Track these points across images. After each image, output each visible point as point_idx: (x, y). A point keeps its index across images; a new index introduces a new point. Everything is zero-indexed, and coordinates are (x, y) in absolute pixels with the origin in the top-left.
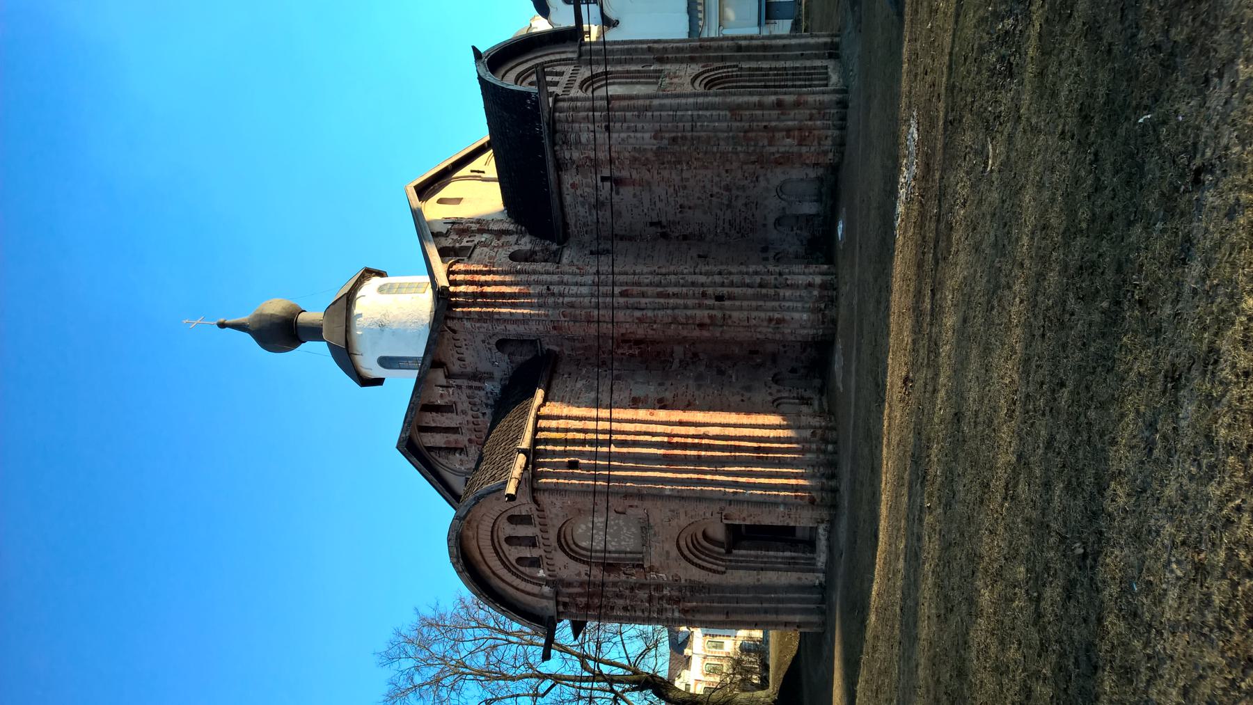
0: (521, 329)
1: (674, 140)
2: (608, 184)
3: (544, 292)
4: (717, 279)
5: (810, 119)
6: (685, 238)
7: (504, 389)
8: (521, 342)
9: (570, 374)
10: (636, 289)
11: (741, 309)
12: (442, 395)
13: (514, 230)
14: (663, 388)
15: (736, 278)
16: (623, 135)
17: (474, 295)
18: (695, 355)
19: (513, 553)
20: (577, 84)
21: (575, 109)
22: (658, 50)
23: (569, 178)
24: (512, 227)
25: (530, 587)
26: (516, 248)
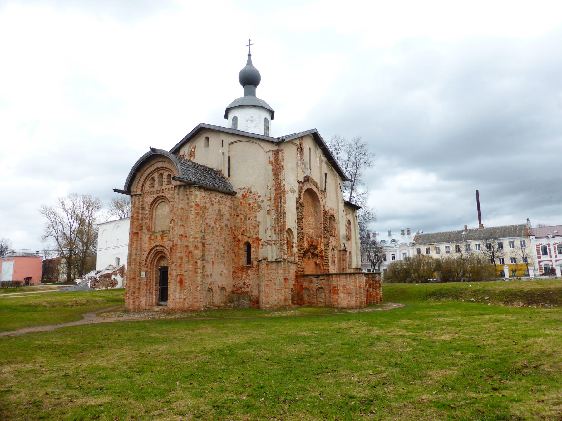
20: (160, 195)
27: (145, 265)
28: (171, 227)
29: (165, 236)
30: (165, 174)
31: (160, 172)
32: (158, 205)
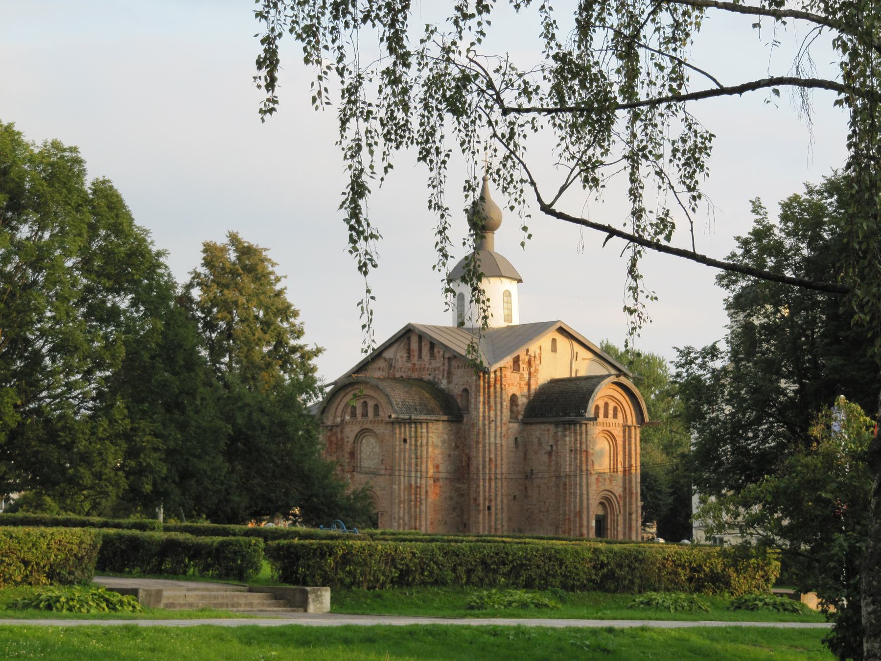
0: (473, 406)
1: (565, 484)
2: (549, 448)
4: (499, 507)
6: (526, 488)
7: (442, 391)
8: (468, 401)
10: (493, 466)
11: (484, 519)
12: (439, 352)
15: (499, 516)
16: (568, 459)
17: (489, 382)
18: (463, 495)
19: (358, 404)
20: (606, 428)
21: (581, 434)
23: (552, 428)
24: (532, 391)
25: (339, 411)
30: (612, 405)
31: (606, 400)
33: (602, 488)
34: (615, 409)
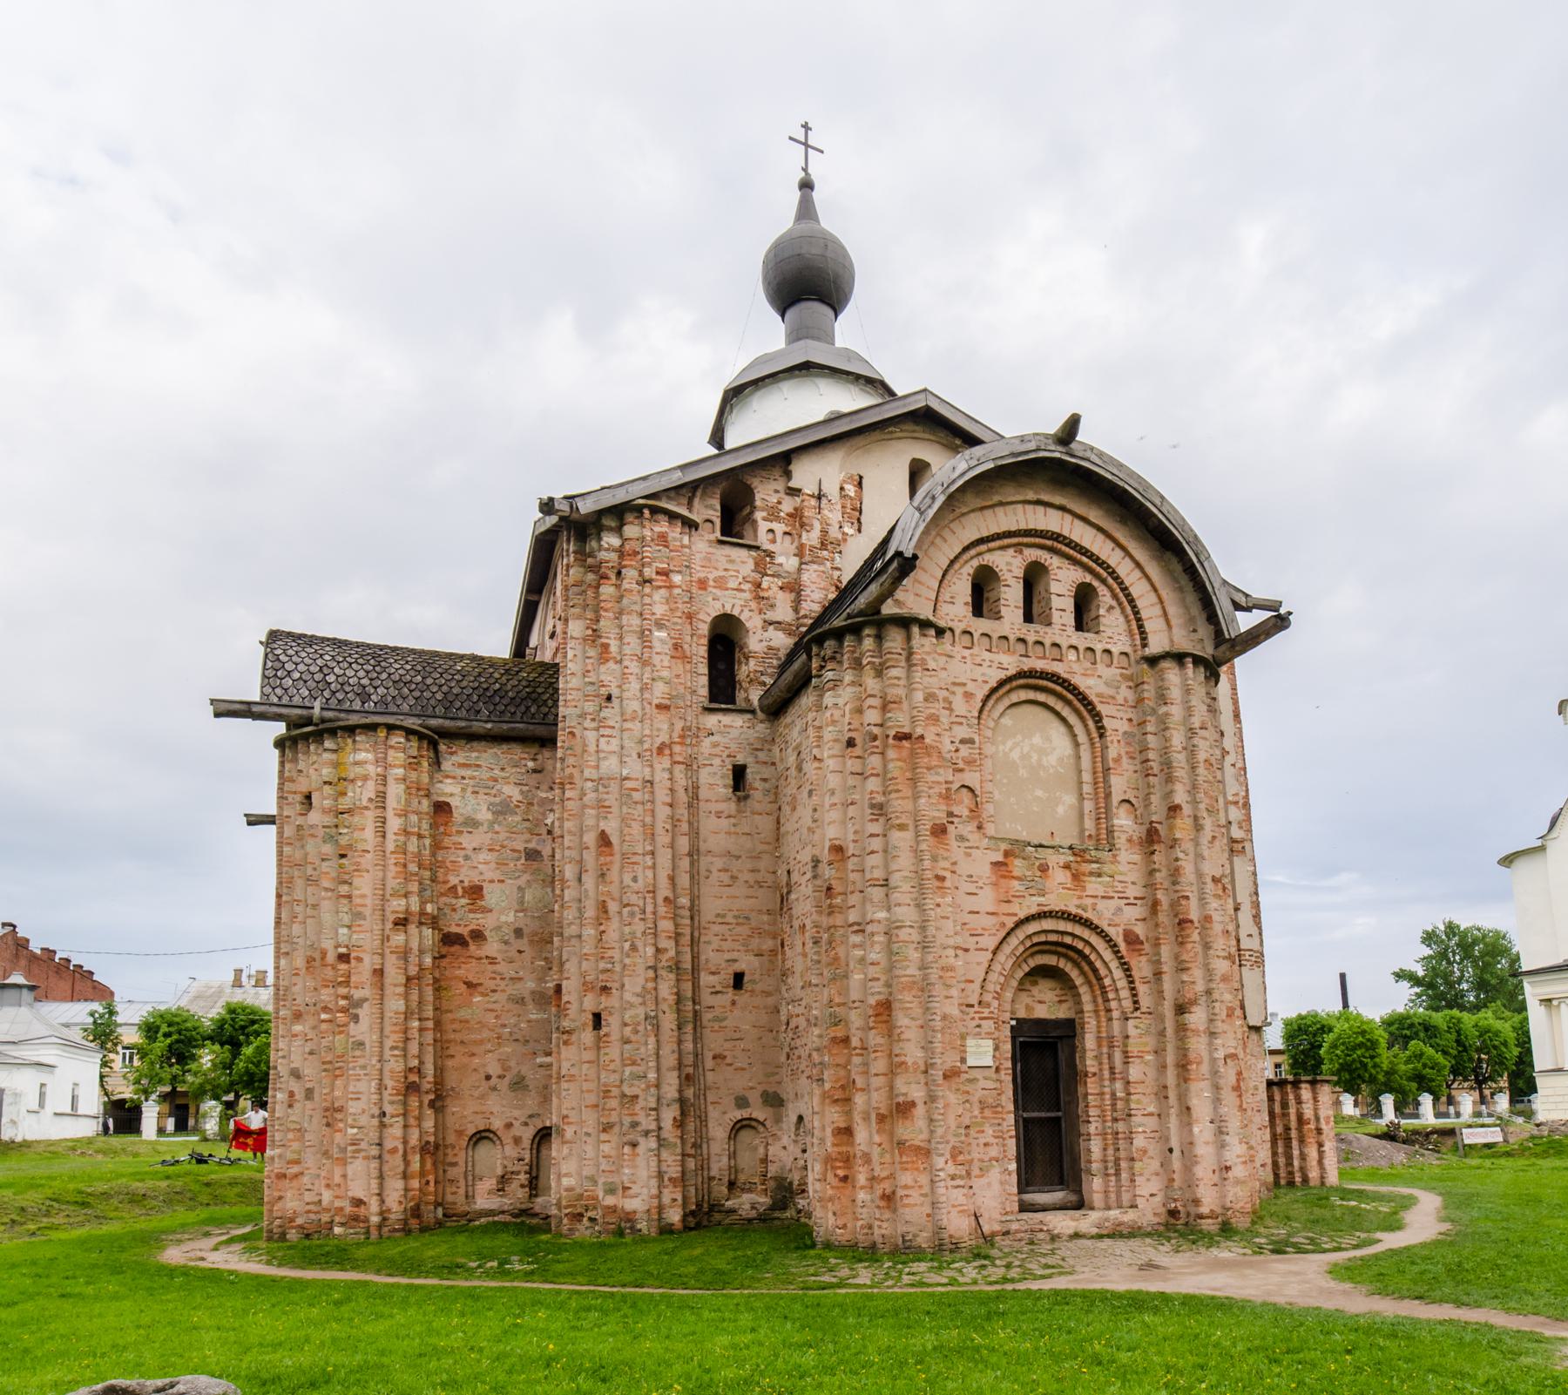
3: (603, 691)
5: (872, 1179)
9: (535, 771)
13: (802, 613)
14: (511, 937)
22: (1171, 828)
26: (752, 620)
27: (980, 1003)
28: (1124, 837)
29: (1091, 874)
32: (1002, 714)
33: (1031, 906)
34: (1083, 600)
